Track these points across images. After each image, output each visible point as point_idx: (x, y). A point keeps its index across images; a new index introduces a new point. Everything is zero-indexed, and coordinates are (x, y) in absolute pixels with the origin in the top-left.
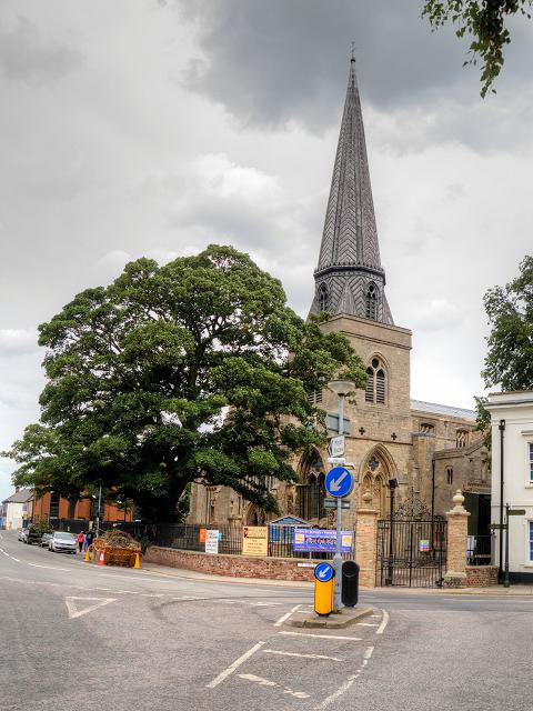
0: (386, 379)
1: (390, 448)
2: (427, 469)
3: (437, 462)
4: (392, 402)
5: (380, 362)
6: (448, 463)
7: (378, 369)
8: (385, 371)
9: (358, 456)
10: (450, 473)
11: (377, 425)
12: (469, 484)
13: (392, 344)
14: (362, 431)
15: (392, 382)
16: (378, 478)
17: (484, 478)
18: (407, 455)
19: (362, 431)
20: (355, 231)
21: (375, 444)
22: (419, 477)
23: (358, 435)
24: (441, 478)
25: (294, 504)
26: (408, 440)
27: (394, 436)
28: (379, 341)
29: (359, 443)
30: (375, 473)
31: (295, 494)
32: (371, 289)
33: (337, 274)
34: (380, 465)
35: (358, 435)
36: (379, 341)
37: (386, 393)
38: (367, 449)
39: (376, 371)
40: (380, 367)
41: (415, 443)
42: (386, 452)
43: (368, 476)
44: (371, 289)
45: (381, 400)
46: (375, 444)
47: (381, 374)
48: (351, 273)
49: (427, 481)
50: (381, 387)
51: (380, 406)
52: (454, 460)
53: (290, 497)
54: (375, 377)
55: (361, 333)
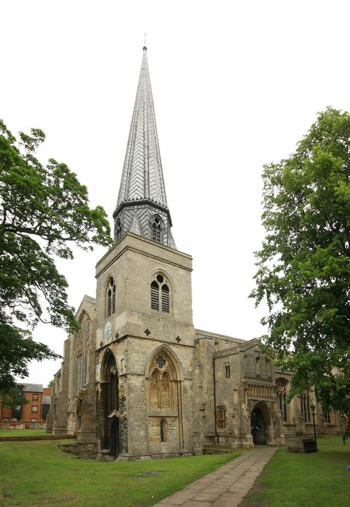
0: (170, 293)
1: (175, 349)
2: (208, 367)
3: (216, 360)
4: (175, 311)
5: (165, 278)
6: (225, 360)
7: (163, 284)
8: (169, 285)
9: (143, 353)
10: (228, 368)
11: (161, 328)
12: (245, 377)
13: (175, 264)
14: (147, 332)
15: (176, 295)
16: (165, 374)
17: (258, 372)
18: (191, 356)
19: (147, 332)
20: (143, 175)
21: (159, 344)
22: (201, 373)
23: (144, 335)
24: (220, 374)
25: (99, 398)
26: (192, 344)
27: (178, 339)
28: (162, 260)
29: (144, 342)
30: (163, 369)
31: (100, 390)
32: (157, 221)
33: (128, 208)
34: (167, 363)
35: (144, 335)
36: (162, 260)
37: (170, 304)
38: (153, 348)
39: (160, 285)
40: (164, 282)
41: (197, 346)
42: (171, 352)
43: (156, 372)
44: (157, 221)
45: (166, 309)
46: (159, 344)
47: (165, 288)
48: (139, 207)
49: (208, 377)
50: (166, 300)
51: (165, 314)
52: (231, 357)
53: (97, 392)
54: (160, 290)
55: (146, 250)
